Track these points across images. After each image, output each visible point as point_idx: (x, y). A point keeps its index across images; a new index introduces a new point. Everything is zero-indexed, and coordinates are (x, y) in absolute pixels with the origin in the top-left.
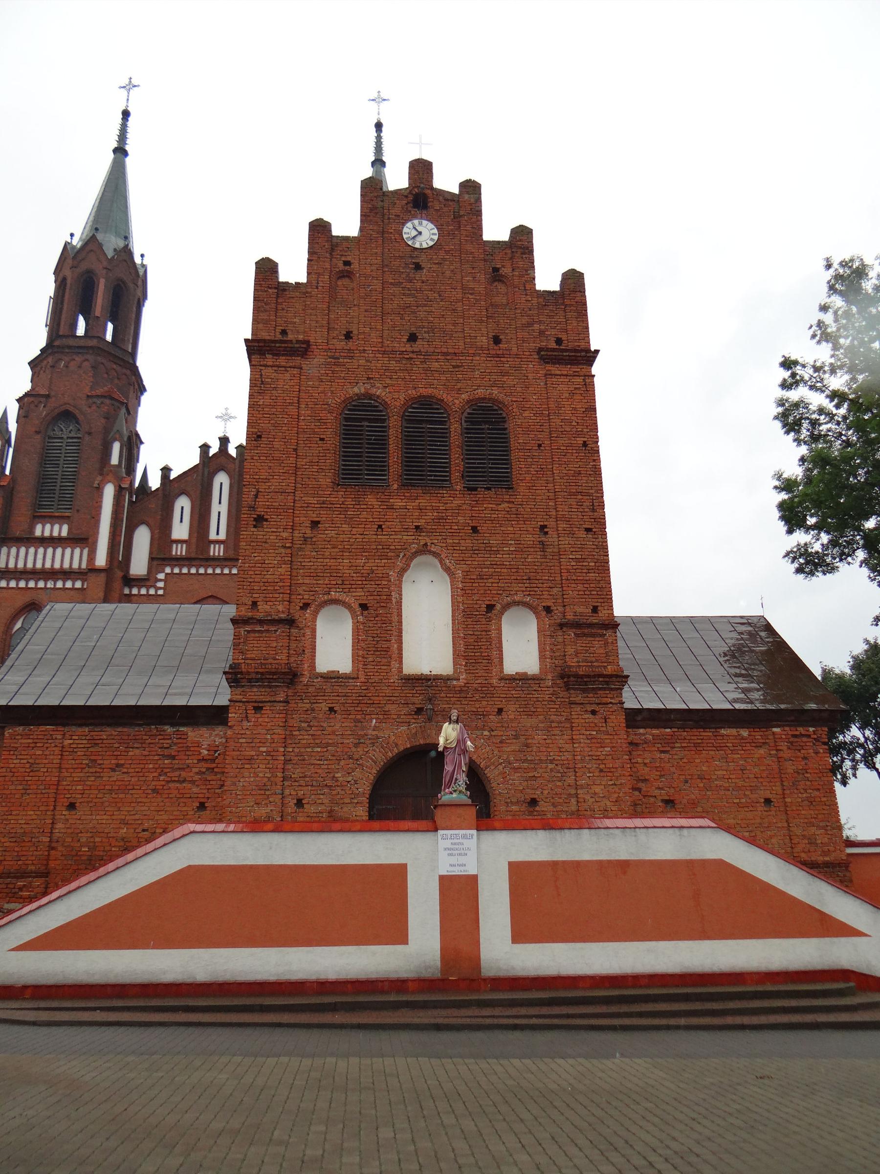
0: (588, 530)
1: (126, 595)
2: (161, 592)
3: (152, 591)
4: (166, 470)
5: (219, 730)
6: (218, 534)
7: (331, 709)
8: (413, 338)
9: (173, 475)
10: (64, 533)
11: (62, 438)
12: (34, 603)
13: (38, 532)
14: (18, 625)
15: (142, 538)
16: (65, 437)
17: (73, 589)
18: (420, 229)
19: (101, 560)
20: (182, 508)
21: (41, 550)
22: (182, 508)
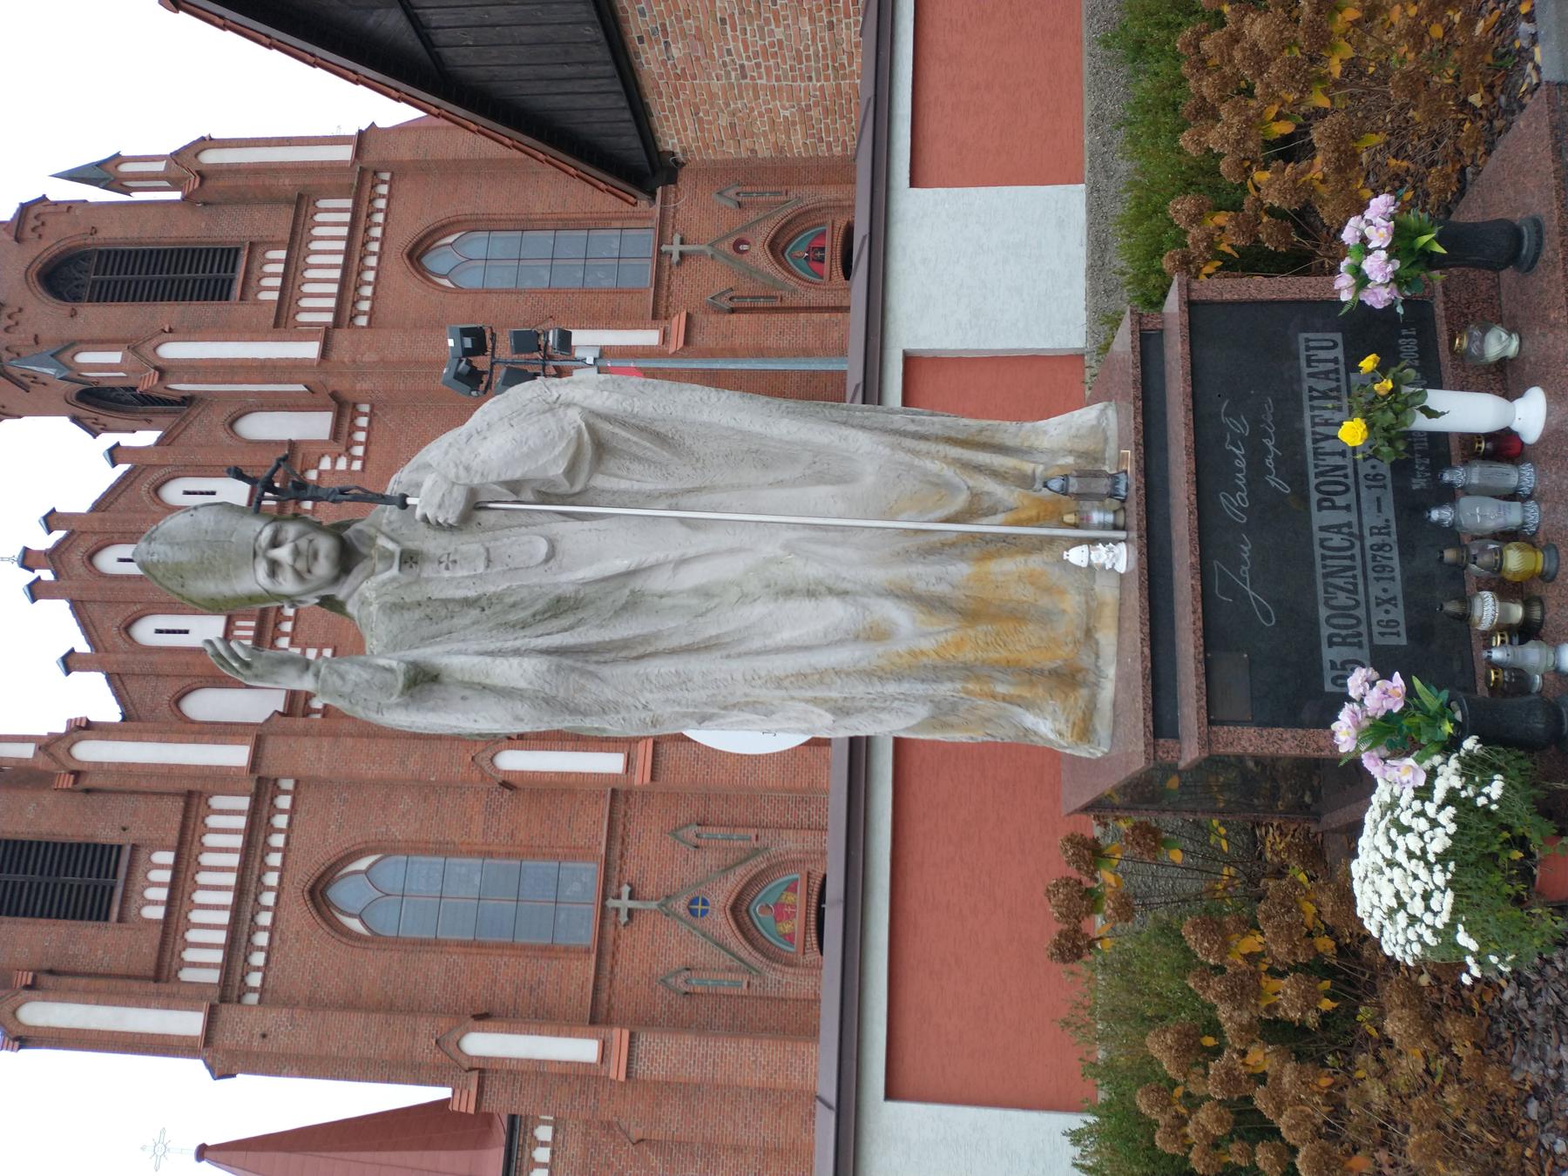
1: (324, 716)
4: (70, 662)
9: (83, 647)
10: (167, 857)
12: (312, 892)
13: (157, 913)
14: (355, 924)
15: (205, 705)
17: (292, 812)
19: (236, 755)
20: (159, 631)
21: (196, 916)
22: (159, 631)
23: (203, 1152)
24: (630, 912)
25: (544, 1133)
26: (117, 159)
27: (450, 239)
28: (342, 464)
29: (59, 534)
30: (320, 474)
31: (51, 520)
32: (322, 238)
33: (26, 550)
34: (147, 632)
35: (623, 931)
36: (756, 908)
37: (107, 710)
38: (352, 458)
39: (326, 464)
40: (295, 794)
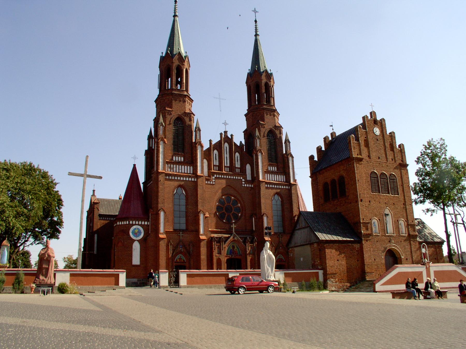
0: (410, 204)
2: (214, 183)
3: (211, 183)
5: (359, 245)
6: (227, 164)
7: (377, 241)
8: (379, 158)
9: (213, 143)
11: (177, 126)
16: (178, 126)
18: (377, 130)
22: (216, 154)
23: (135, 165)
24: (180, 236)
25: (146, 223)
26: (289, 142)
27: (280, 198)
28: (243, 183)
29: (230, 137)
30: (242, 179)
31: (232, 135)
32: (279, 177)
33: (227, 132)
34: (216, 152)
35: (177, 234)
36: (180, 255)
37: (204, 149)
38: (244, 184)
39: (243, 180)
40: (194, 181)
